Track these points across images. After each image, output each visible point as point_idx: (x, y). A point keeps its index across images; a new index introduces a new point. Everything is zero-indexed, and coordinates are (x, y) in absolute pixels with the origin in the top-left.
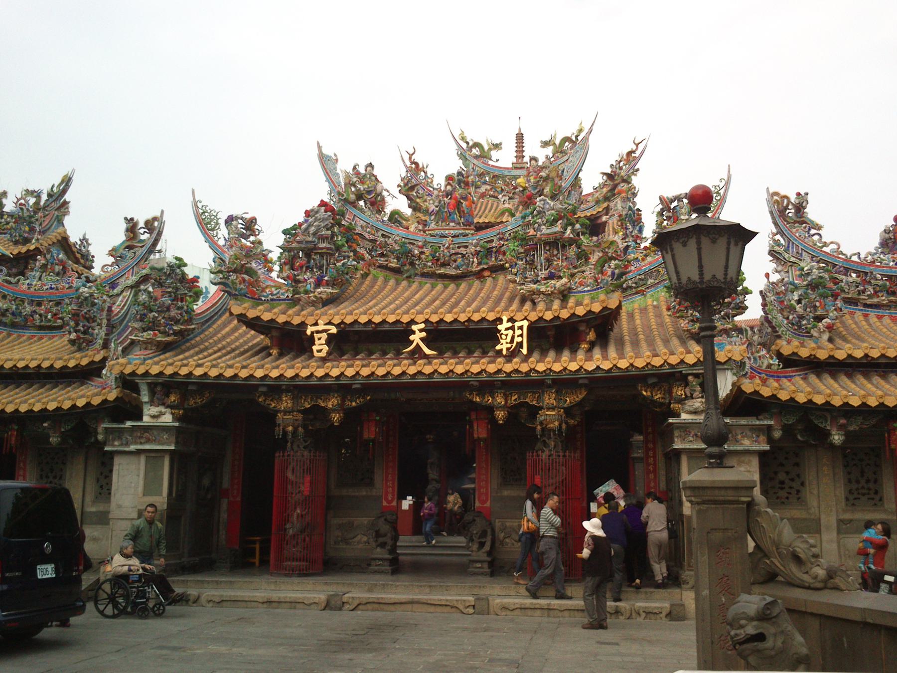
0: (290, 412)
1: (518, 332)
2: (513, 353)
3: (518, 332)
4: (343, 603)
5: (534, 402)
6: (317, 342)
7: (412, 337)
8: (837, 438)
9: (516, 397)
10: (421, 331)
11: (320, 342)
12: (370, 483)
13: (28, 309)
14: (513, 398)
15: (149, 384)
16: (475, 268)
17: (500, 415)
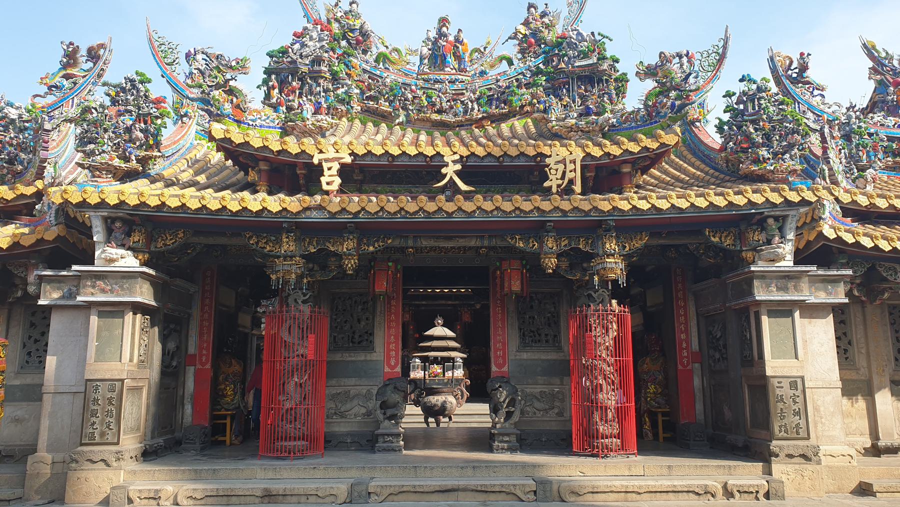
0: (291, 257)
1: (572, 167)
2: (567, 191)
3: (571, 167)
4: (369, 493)
5: (588, 249)
6: (326, 172)
7: (444, 171)
9: (567, 242)
10: (454, 162)
11: (330, 173)
15: (105, 219)
16: (477, 114)
17: (551, 263)
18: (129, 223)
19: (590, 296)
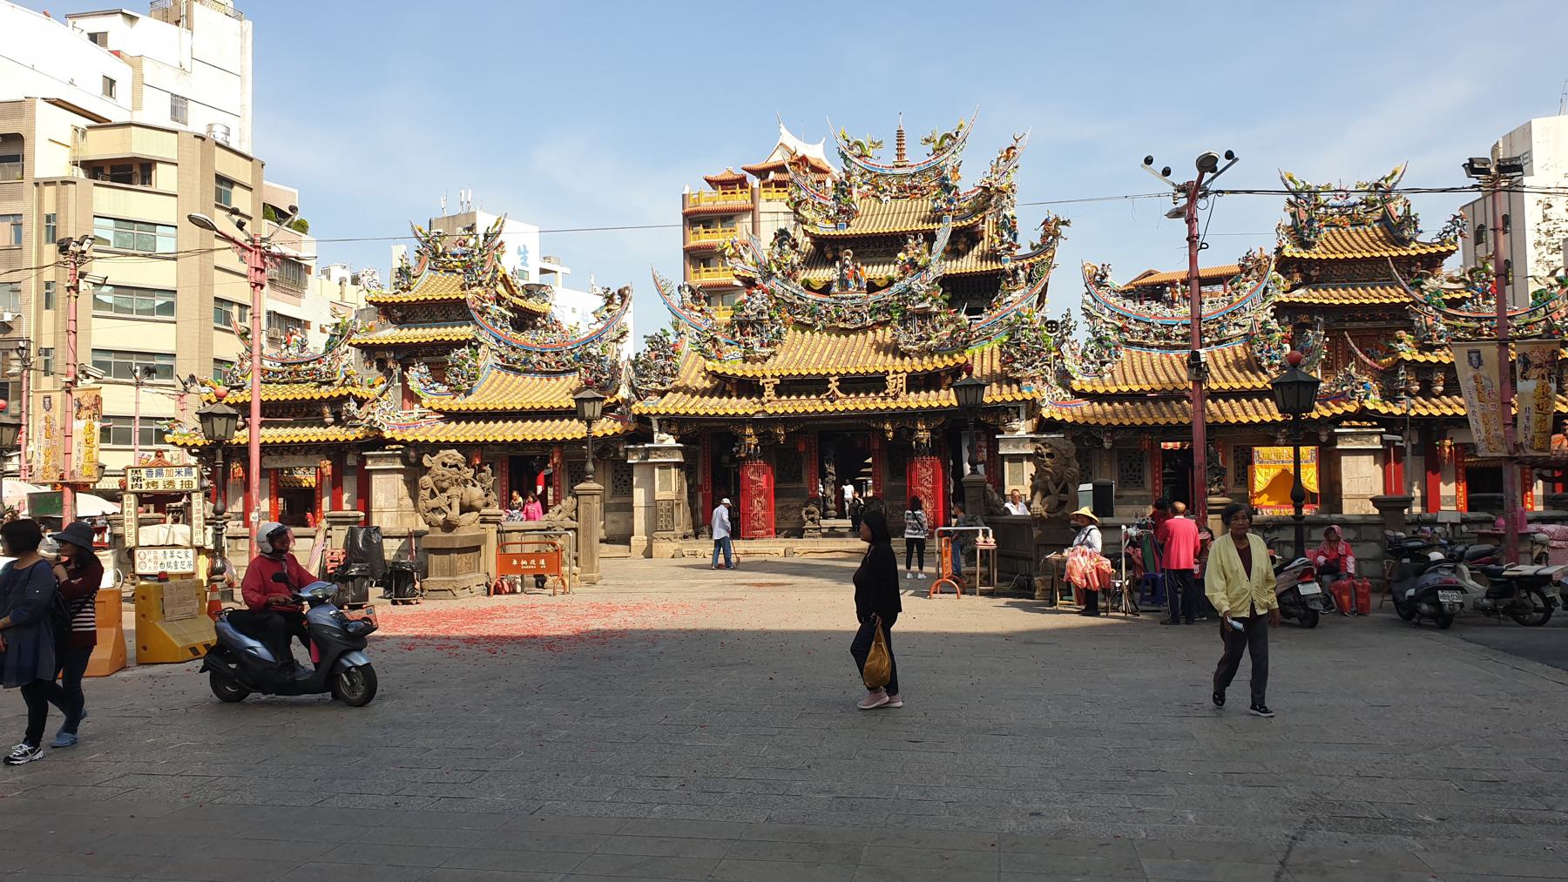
8: (1107, 445)
12: (800, 480)
13: (535, 359)
18: (670, 422)
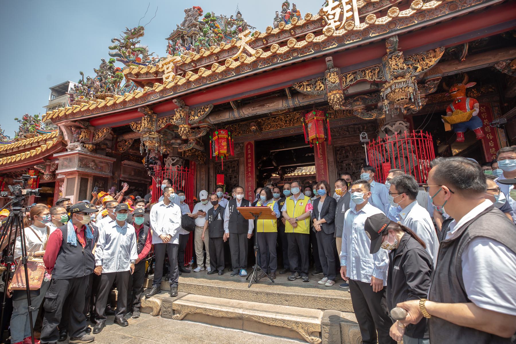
3: (347, 7)
4: (174, 310)
5: (375, 78)
14: (348, 80)
15: (67, 127)
19: (387, 131)
